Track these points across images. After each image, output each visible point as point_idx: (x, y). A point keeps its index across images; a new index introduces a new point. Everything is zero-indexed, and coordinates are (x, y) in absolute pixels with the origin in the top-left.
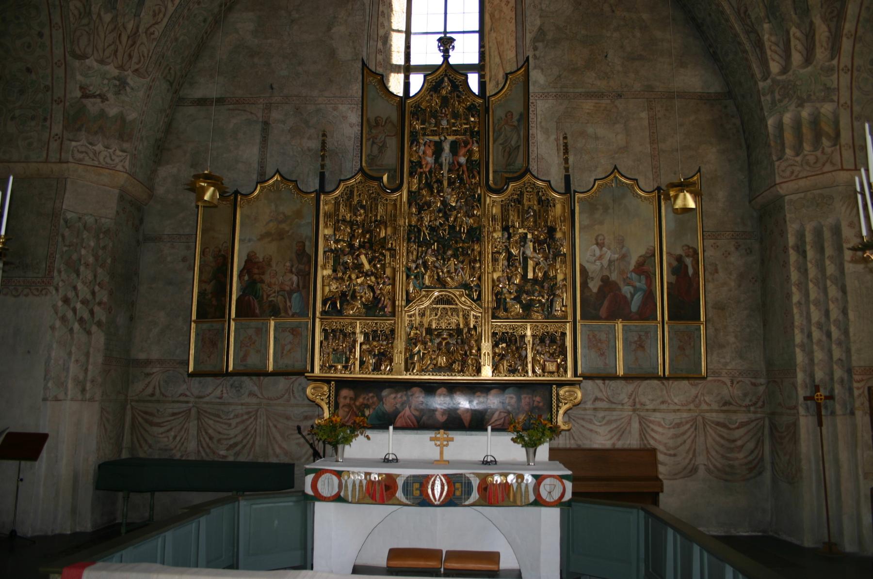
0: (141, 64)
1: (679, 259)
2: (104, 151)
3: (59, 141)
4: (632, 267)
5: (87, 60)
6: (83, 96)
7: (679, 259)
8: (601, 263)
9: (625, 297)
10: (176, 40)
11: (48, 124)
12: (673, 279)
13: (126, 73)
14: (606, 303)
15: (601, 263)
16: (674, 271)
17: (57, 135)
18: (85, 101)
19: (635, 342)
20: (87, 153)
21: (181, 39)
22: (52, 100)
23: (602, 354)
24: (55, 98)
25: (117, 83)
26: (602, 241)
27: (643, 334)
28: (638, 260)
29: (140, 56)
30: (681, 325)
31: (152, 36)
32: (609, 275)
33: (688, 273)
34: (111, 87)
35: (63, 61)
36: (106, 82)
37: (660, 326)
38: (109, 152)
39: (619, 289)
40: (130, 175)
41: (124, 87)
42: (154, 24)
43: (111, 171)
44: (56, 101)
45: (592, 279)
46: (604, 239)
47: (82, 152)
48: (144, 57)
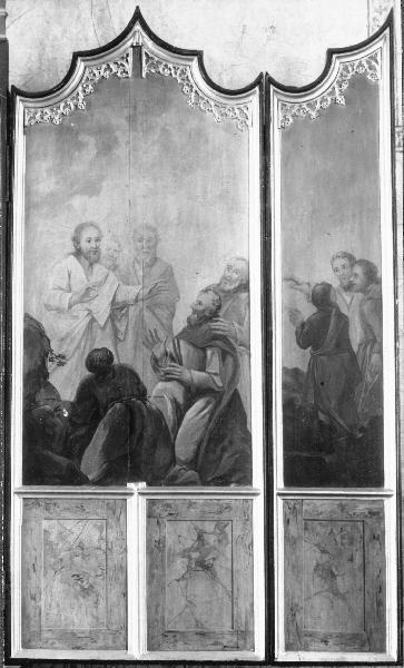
1: (322, 297)
4: (180, 324)
7: (322, 297)
8: (90, 312)
9: (158, 417)
12: (301, 360)
14: (101, 435)
15: (90, 312)
16: (308, 335)
19: (185, 553)
23: (86, 592)
26: (93, 244)
27: (209, 527)
28: (200, 303)
30: (322, 499)
32: (111, 349)
33: (348, 341)
37: (258, 505)
39: (143, 394)
45: (62, 360)
46: (98, 240)
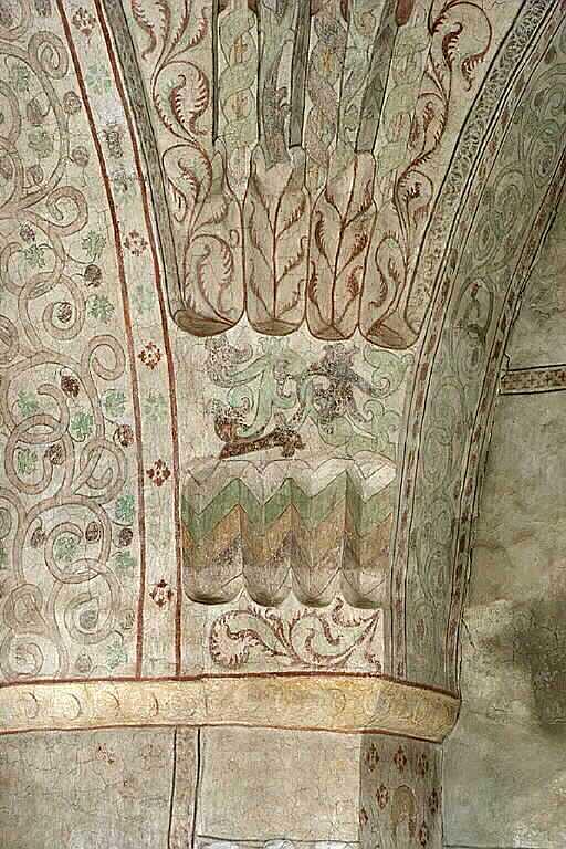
0: (384, 308)
2: (306, 615)
3: (170, 607)
5: (229, 333)
6: (226, 448)
10: (488, 195)
11: (134, 549)
13: (347, 344)
17: (162, 584)
18: (235, 464)
20: (255, 636)
21: (500, 189)
22: (141, 470)
24: (148, 466)
25: (325, 383)
29: (383, 279)
31: (415, 204)
34: (308, 399)
35: (161, 346)
36: (290, 387)
38: (321, 618)
40: (392, 679)
41: (347, 392)
42: (415, 163)
43: (332, 682)
44: (151, 473)
47: (240, 635)
48: (394, 275)
